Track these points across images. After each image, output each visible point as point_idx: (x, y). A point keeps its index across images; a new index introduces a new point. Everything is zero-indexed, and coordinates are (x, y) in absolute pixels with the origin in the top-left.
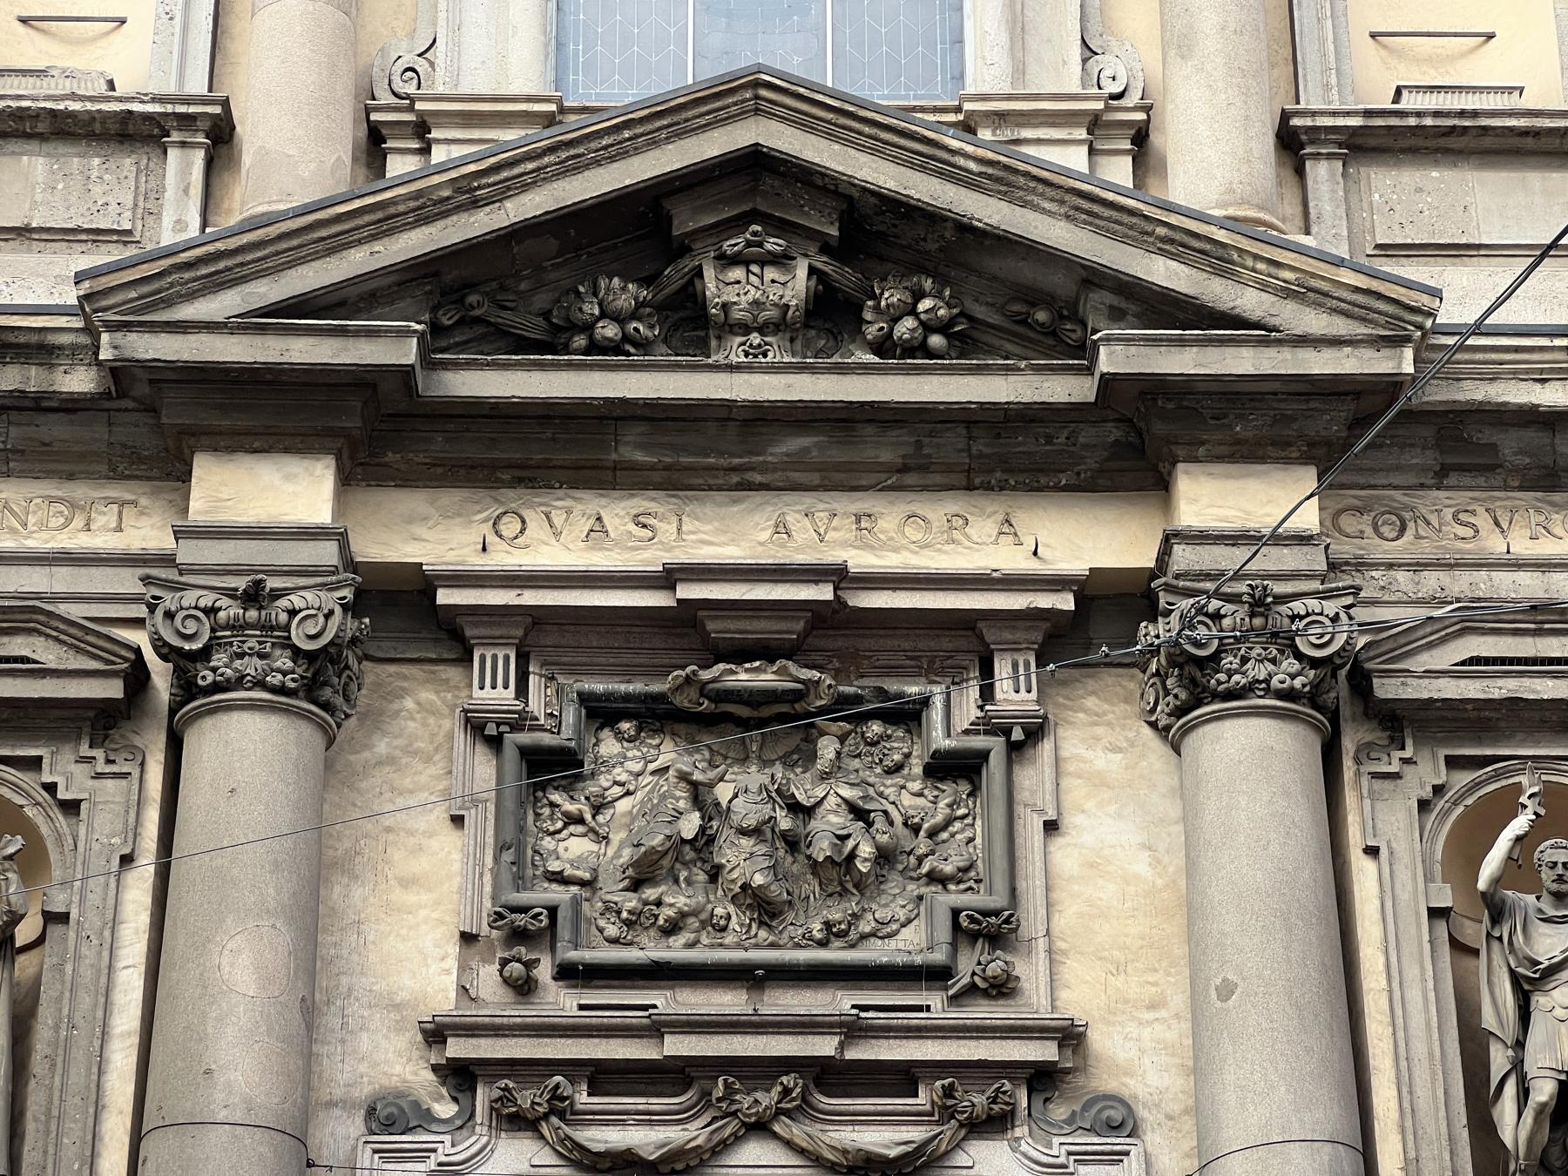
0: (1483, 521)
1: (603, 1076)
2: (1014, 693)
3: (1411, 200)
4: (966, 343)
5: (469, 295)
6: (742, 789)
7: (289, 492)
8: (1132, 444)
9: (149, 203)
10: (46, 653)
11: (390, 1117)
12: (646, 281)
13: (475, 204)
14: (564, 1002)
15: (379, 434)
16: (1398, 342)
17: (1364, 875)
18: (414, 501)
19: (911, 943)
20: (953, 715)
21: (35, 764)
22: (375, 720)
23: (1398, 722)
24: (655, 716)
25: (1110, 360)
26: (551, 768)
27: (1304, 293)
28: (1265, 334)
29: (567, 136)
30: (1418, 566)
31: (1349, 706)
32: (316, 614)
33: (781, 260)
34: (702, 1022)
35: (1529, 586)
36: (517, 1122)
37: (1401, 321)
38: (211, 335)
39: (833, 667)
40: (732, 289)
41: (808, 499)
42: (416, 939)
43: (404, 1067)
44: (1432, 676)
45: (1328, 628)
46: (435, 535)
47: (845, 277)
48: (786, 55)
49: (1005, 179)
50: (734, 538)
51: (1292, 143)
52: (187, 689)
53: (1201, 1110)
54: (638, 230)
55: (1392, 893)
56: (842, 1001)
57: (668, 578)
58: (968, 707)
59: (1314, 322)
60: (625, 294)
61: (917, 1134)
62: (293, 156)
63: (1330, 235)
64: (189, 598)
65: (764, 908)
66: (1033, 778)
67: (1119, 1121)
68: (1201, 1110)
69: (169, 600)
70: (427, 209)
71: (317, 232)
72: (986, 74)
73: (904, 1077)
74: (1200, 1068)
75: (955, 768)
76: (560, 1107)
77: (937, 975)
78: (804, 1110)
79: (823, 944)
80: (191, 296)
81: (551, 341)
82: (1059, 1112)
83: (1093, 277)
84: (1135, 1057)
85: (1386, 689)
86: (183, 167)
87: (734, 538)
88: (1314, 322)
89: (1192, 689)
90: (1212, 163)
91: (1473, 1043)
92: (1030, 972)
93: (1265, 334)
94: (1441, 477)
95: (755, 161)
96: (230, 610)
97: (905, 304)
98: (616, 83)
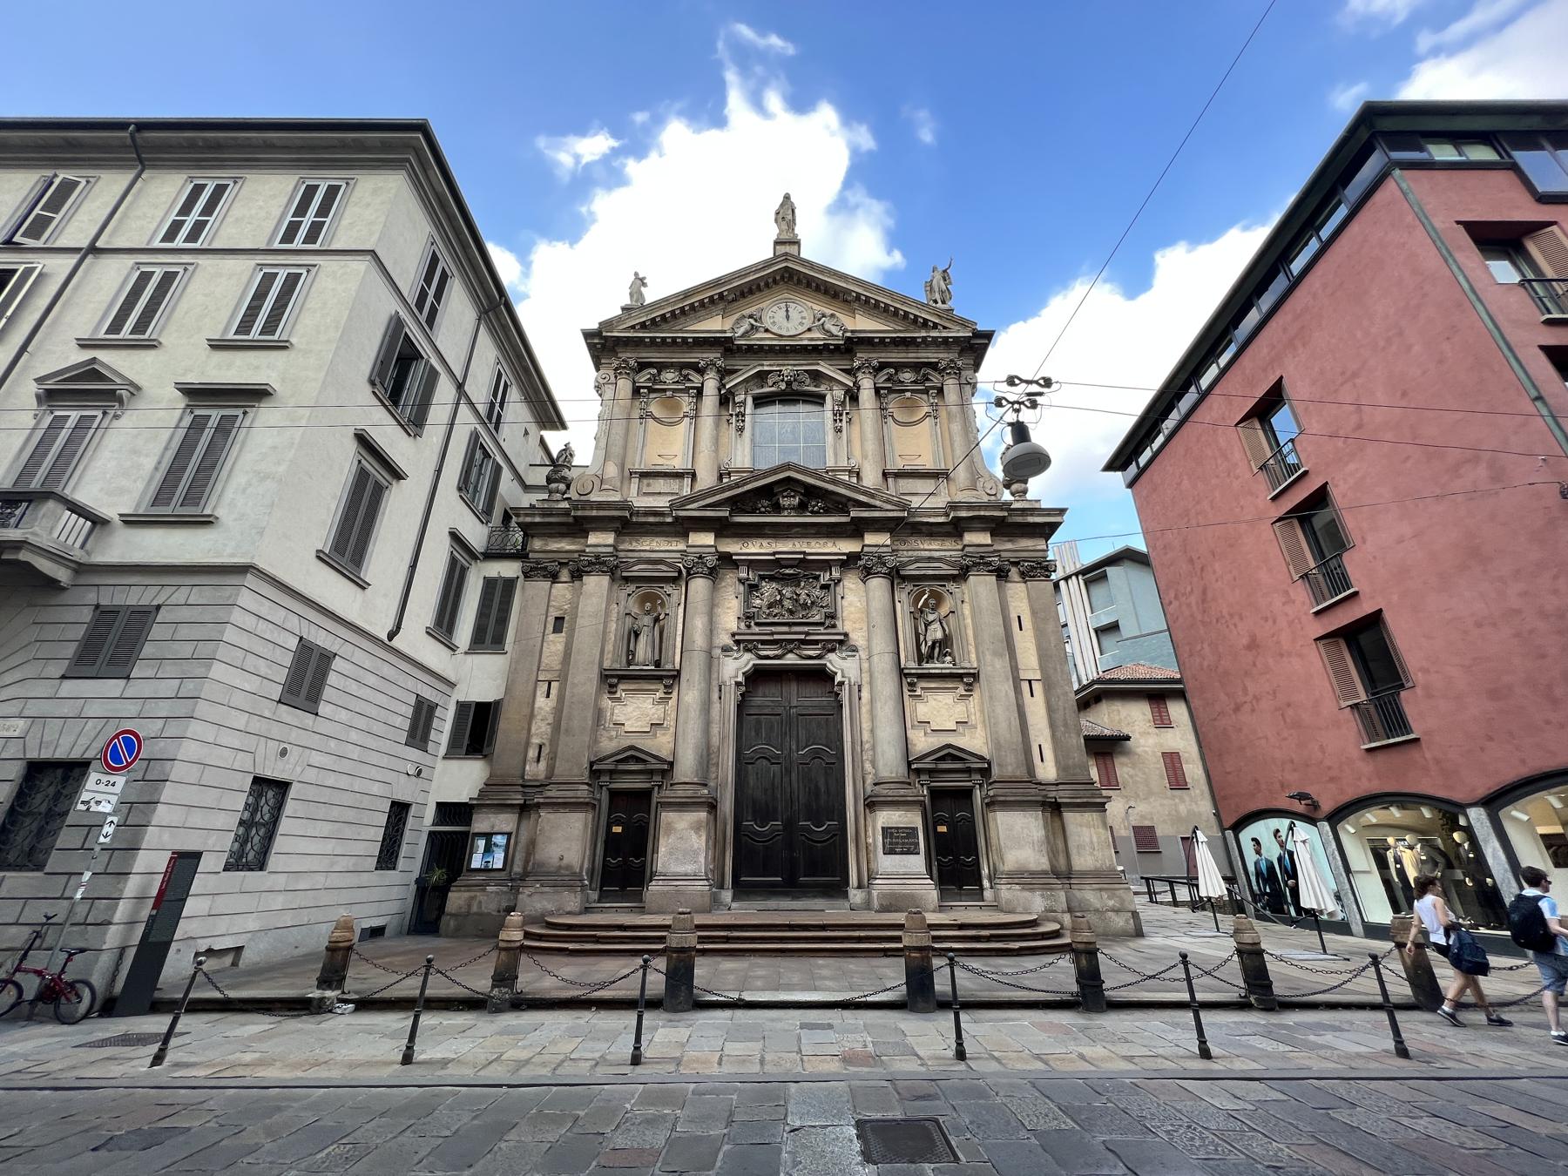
1: (763, 642)
2: (836, 574)
3: (906, 485)
4: (827, 511)
5: (740, 503)
6: (787, 591)
7: (707, 539)
8: (856, 529)
9: (681, 488)
10: (664, 568)
11: (726, 649)
14: (756, 629)
15: (722, 528)
17: (898, 606)
20: (825, 578)
22: (722, 579)
23: (905, 578)
24: (772, 578)
25: (852, 514)
26: (753, 588)
27: (888, 502)
28: (881, 509)
29: (755, 475)
31: (896, 576)
32: (711, 561)
34: (781, 633)
35: (927, 554)
37: (904, 507)
38: (692, 511)
40: (785, 502)
42: (730, 618)
43: (729, 641)
44: (911, 570)
45: (891, 561)
46: (732, 547)
48: (794, 459)
51: (885, 475)
52: (689, 574)
53: (869, 647)
54: (768, 492)
55: (903, 609)
56: (806, 629)
57: (774, 554)
58: (827, 576)
59: (889, 507)
60: (766, 503)
62: (706, 480)
63: (892, 491)
65: (791, 612)
66: (839, 589)
67: (855, 650)
68: (869, 647)
70: (730, 488)
71: (710, 492)
72: (830, 463)
73: (816, 642)
74: (869, 640)
75: (824, 587)
76: (756, 648)
77: (822, 624)
81: (753, 511)
83: (850, 499)
84: (857, 638)
86: (687, 481)
88: (889, 507)
89: (868, 573)
90: (871, 479)
91: (917, 635)
92: (839, 624)
93: (881, 509)
94: (912, 535)
95: (789, 479)
98: (764, 466)
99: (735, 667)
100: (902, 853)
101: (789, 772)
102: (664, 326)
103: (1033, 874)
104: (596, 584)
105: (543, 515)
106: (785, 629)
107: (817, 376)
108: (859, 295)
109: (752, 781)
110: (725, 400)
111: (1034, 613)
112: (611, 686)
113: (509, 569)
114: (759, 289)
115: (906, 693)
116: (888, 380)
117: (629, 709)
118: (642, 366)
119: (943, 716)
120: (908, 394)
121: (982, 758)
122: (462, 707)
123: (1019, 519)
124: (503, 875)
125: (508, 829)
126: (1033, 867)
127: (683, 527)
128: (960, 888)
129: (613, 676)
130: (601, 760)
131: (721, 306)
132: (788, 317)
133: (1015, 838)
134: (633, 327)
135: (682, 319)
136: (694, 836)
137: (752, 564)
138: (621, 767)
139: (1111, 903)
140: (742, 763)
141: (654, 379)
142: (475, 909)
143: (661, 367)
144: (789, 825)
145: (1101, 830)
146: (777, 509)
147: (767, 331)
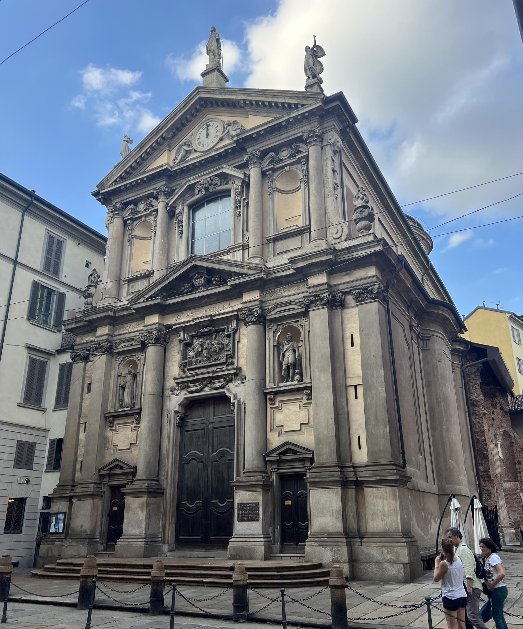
0: (282, 291)
7: (154, 319)
8: (236, 292)
12: (190, 283)
13: (165, 280)
14: (188, 373)
15: (162, 310)
16: (261, 272)
17: (267, 342)
18: (169, 316)
19: (224, 360)
21: (135, 355)
27: (251, 268)
30: (274, 300)
33: (201, 277)
36: (183, 389)
39: (214, 327)
40: (197, 282)
41: (208, 306)
44: (273, 315)
46: (172, 320)
47: (209, 277)
49: (219, 262)
50: (201, 314)
59: (252, 272)
61: (222, 383)
64: (144, 334)
69: (142, 335)
76: (188, 387)
78: (210, 383)
79: (215, 361)
80: (140, 299)
82: (238, 378)
85: (268, 318)
87: (201, 314)
88: (252, 272)
95: (194, 266)
96: (148, 335)
97: (215, 280)
99: (175, 401)
100: (248, 520)
101: (207, 467)
102: (135, 172)
103: (330, 535)
104: (100, 361)
105: (76, 323)
106: (204, 370)
107: (225, 177)
108: (245, 101)
109: (187, 475)
110: (171, 213)
111: (361, 331)
112: (110, 423)
113: (66, 358)
114: (188, 121)
115: (269, 406)
116: (272, 162)
117: (120, 436)
118: (126, 205)
119: (296, 422)
120: (287, 168)
121: (308, 450)
122: (52, 441)
123: (347, 257)
124: (63, 536)
125: (64, 511)
126: (331, 529)
127: (141, 314)
128: (297, 545)
129: (110, 417)
130: (103, 468)
131: (166, 144)
132: (208, 135)
133: (324, 507)
134: (115, 181)
135: (144, 163)
136: (140, 513)
137: (185, 329)
138: (113, 472)
139: (389, 557)
140: (182, 463)
141: (134, 212)
142: (50, 554)
143: (136, 203)
144: (206, 502)
145: (392, 501)
146: (194, 288)
147: (195, 151)
